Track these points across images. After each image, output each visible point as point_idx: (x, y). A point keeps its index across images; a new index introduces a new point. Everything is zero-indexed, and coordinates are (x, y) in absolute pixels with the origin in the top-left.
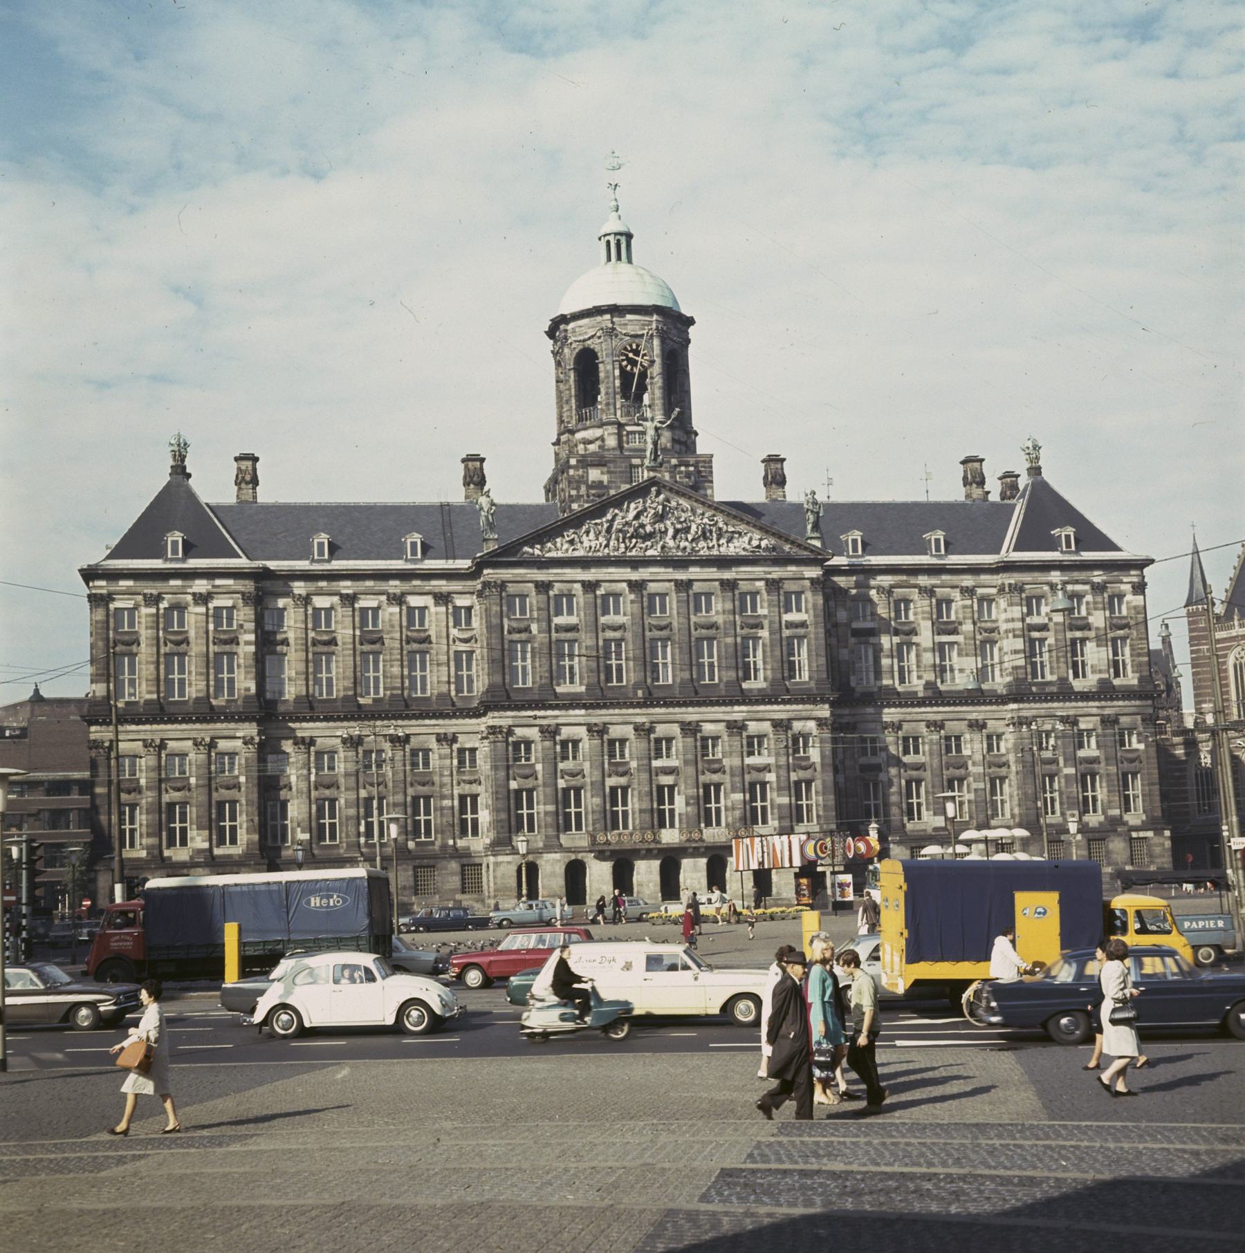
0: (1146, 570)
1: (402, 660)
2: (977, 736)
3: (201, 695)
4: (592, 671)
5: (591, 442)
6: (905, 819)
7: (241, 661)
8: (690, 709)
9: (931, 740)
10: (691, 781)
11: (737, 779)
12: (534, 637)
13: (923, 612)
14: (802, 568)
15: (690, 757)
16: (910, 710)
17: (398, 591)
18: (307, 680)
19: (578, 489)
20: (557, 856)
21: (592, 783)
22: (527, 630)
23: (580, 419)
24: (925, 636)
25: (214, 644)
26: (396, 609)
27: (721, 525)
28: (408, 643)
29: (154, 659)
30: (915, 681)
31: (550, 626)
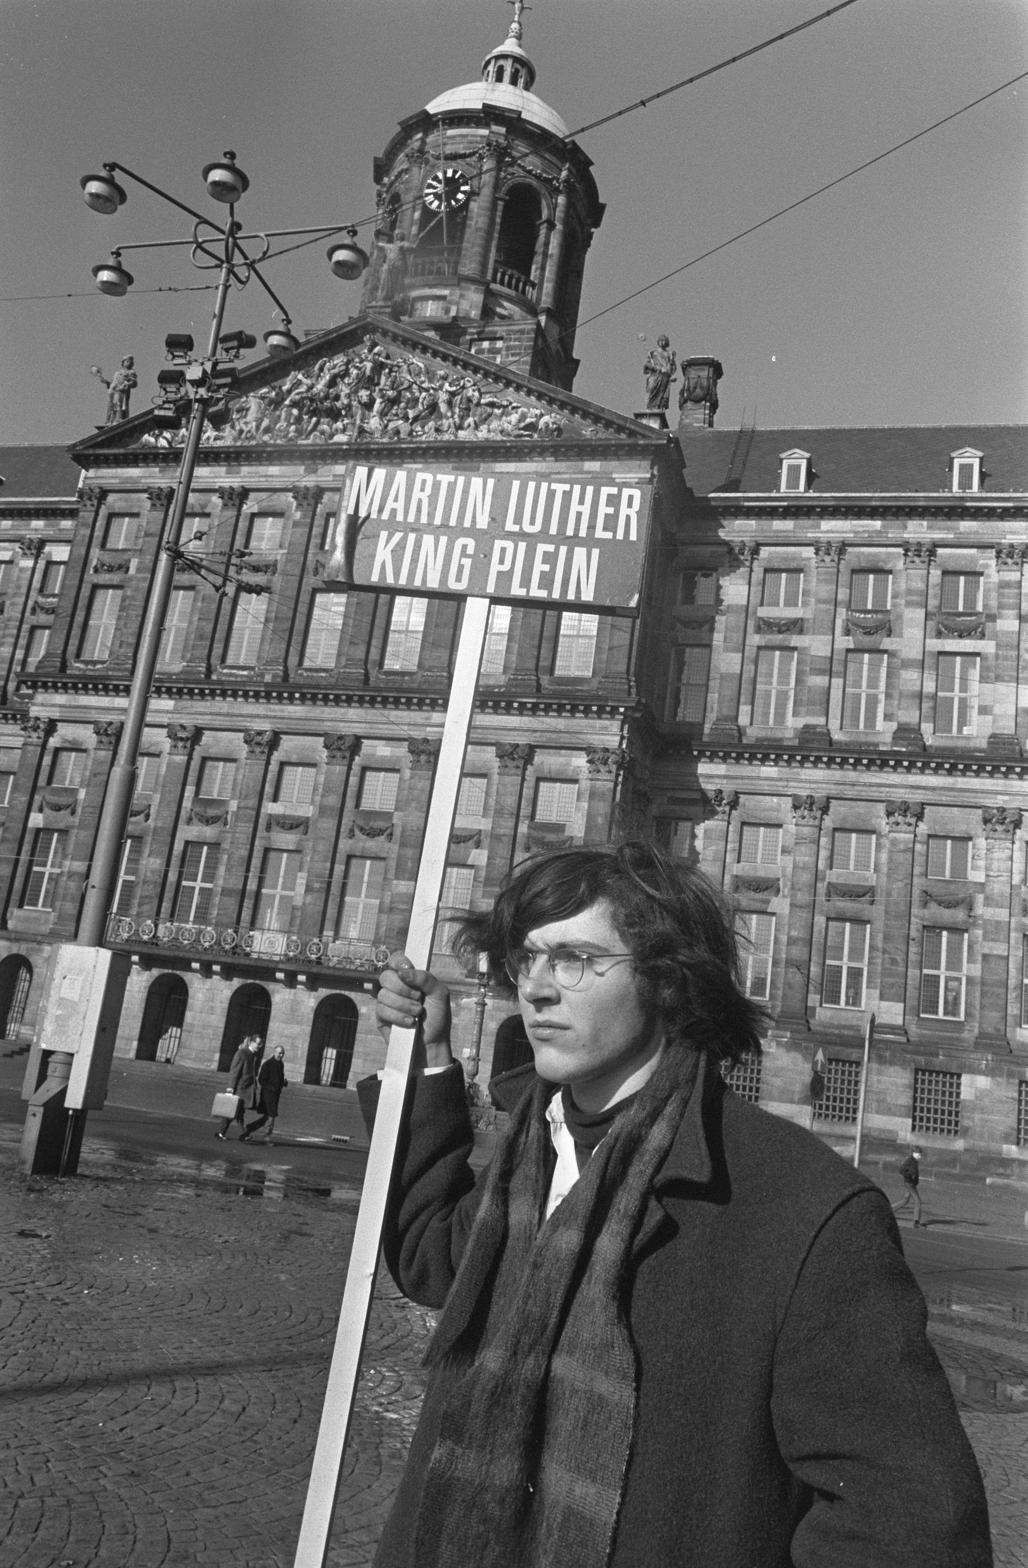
6: (813, 999)
8: (353, 712)
9: (894, 843)
10: (324, 847)
12: (131, 579)
13: (909, 592)
14: (614, 464)
15: (333, 800)
16: (851, 775)
17: (35, 536)
21: (155, 829)
22: (124, 567)
24: (912, 637)
26: (29, 563)
27: (470, 393)
28: (34, 611)
30: (880, 724)
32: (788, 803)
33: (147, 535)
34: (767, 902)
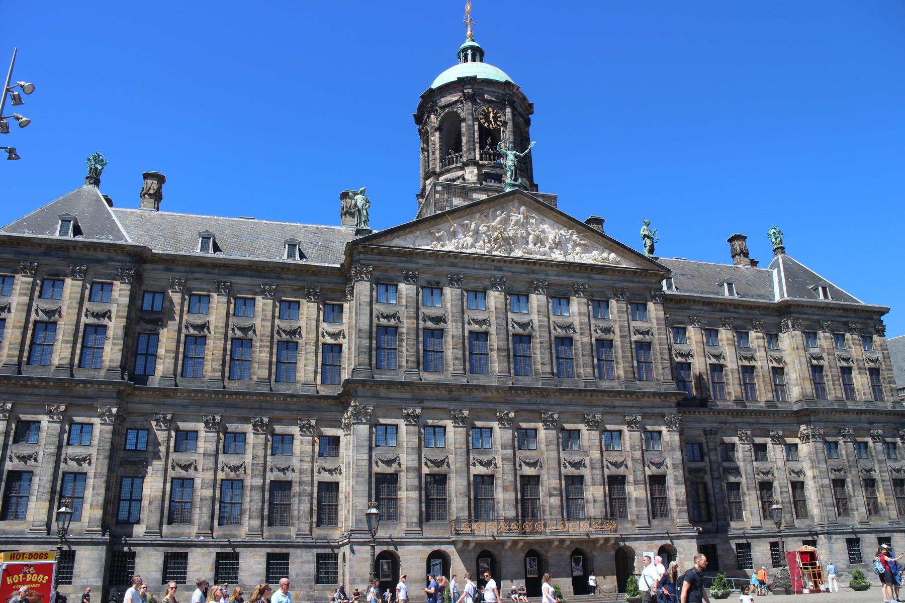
0: (882, 318)
1: (271, 348)
2: (779, 448)
3: (64, 362)
4: (457, 359)
5: (454, 180)
7: (110, 333)
11: (598, 472)
13: (728, 339)
18: (176, 359)
19: (443, 208)
20: (420, 547)
23: (445, 161)
25: (86, 315)
29: (22, 324)
31: (417, 313)
32: (702, 434)
33: (407, 297)
34: (703, 478)
